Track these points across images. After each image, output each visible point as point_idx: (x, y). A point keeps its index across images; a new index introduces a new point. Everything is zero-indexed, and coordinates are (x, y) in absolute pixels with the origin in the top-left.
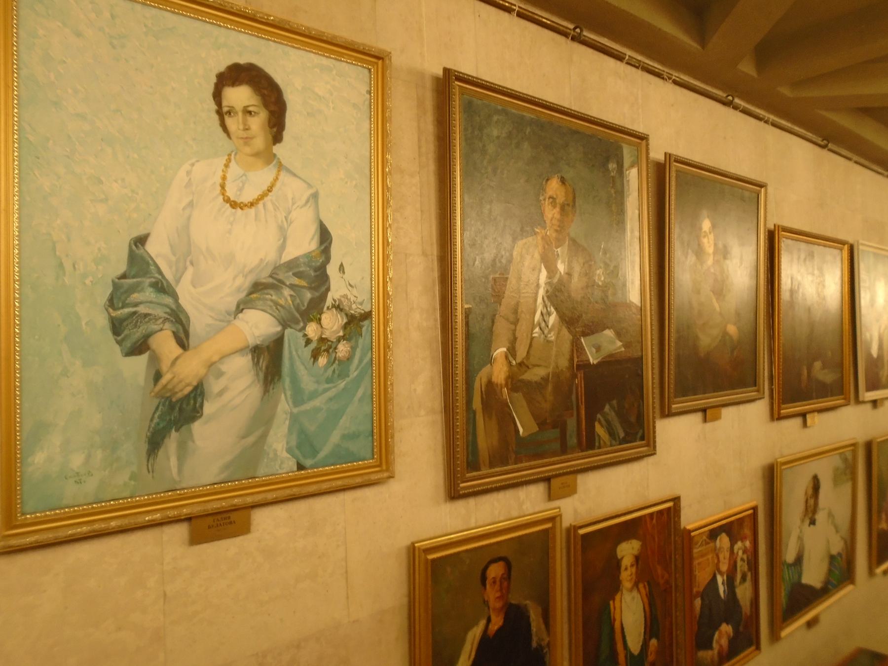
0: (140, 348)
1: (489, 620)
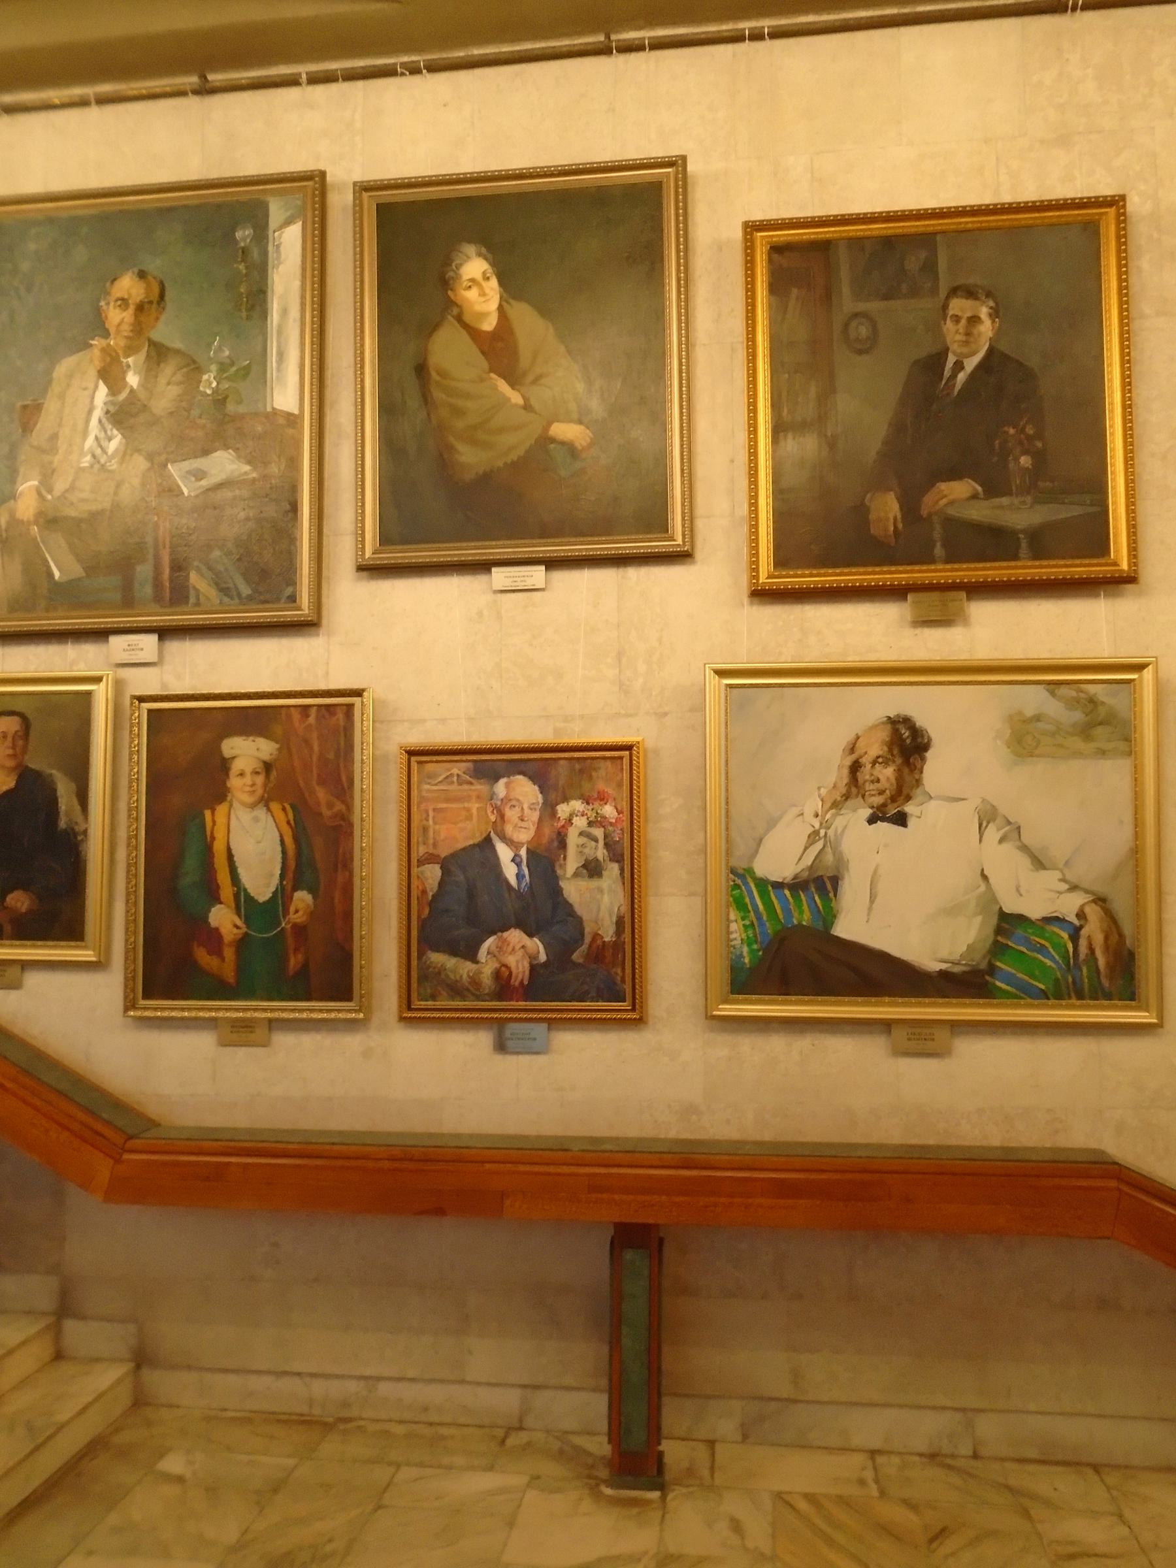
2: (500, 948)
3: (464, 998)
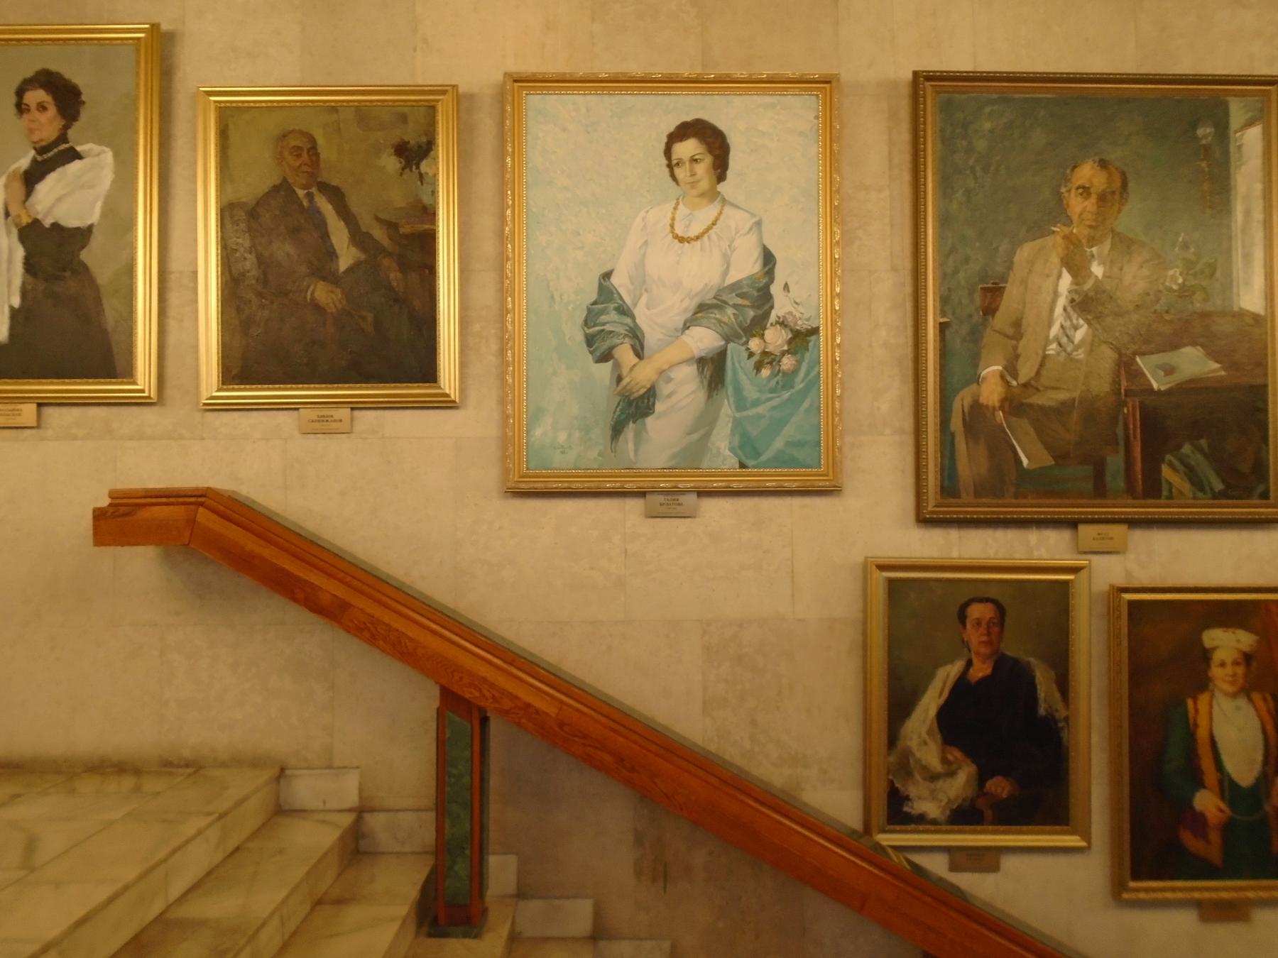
0: (605, 357)
1: (970, 663)
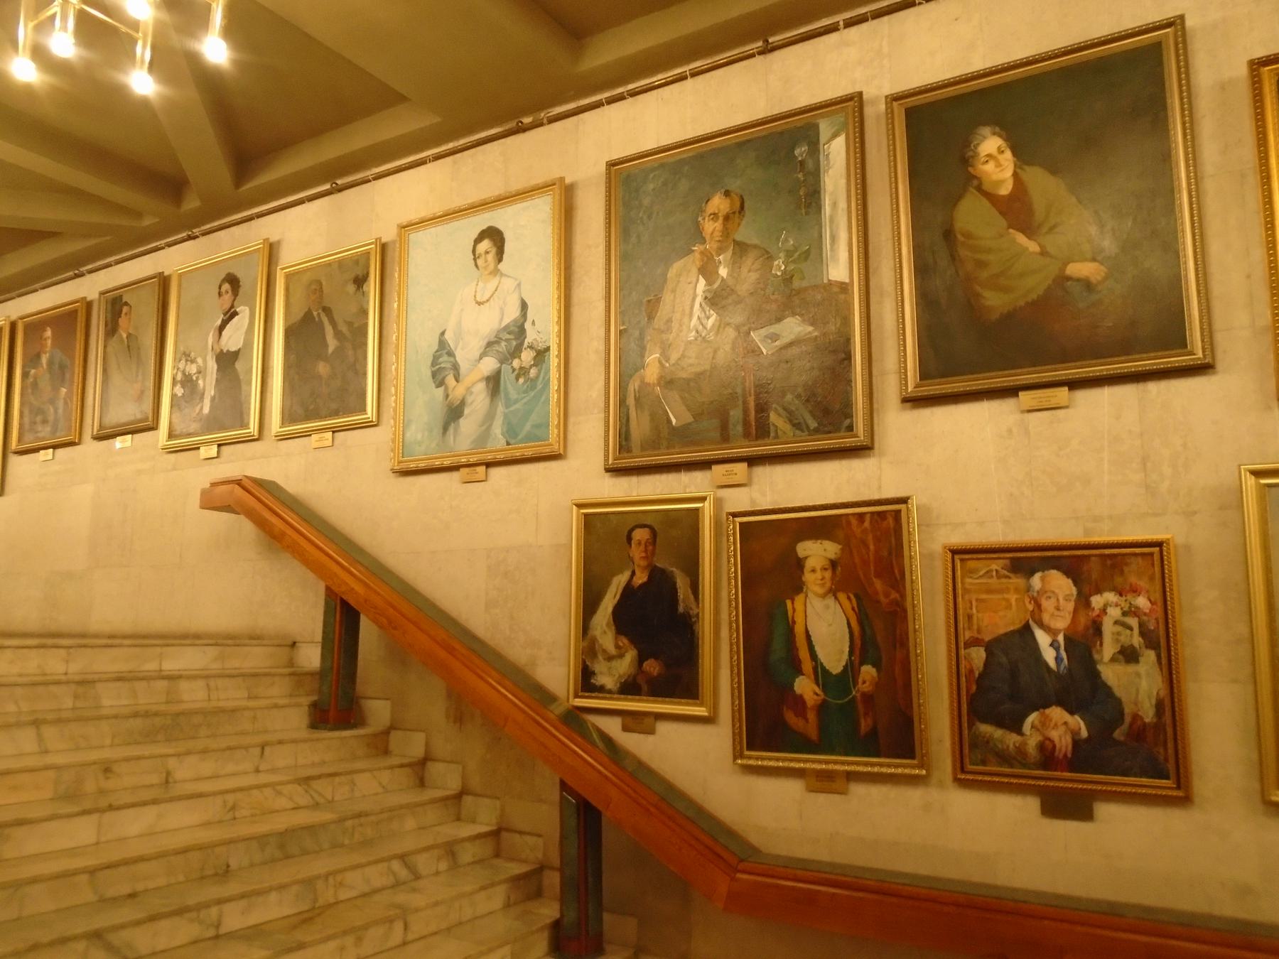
0: (441, 384)
1: (633, 573)
2: (1043, 724)
3: (1011, 766)
